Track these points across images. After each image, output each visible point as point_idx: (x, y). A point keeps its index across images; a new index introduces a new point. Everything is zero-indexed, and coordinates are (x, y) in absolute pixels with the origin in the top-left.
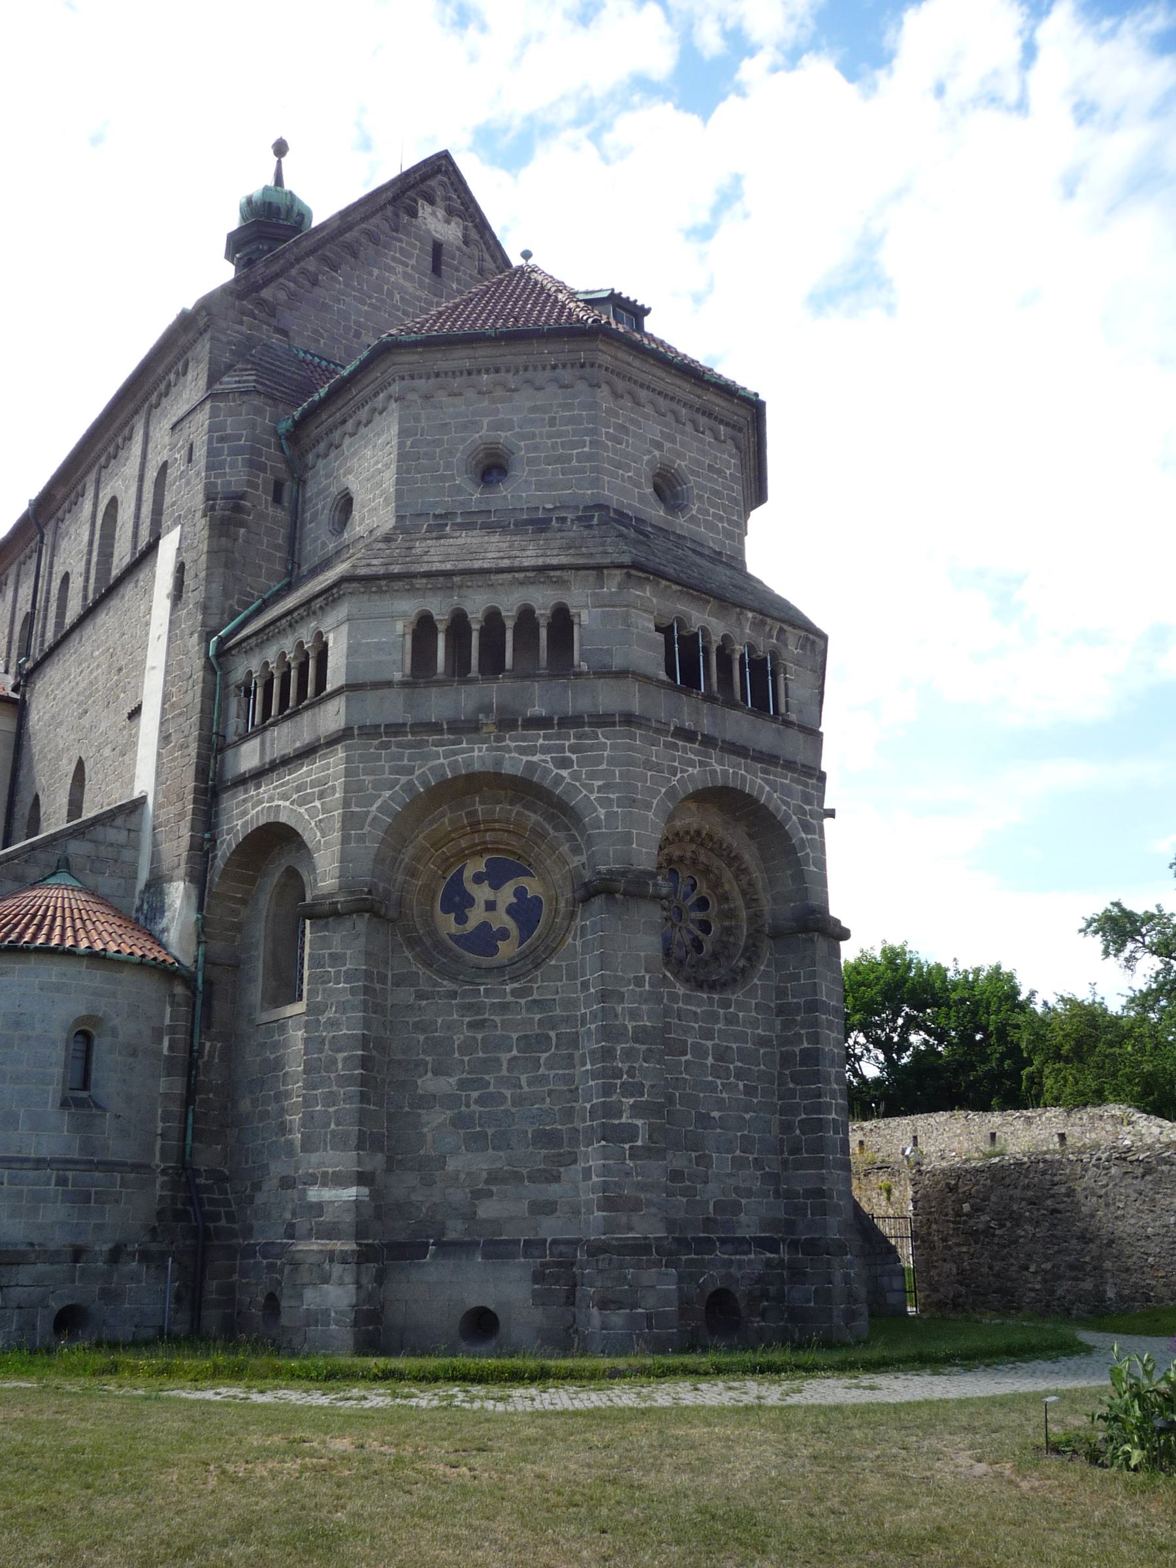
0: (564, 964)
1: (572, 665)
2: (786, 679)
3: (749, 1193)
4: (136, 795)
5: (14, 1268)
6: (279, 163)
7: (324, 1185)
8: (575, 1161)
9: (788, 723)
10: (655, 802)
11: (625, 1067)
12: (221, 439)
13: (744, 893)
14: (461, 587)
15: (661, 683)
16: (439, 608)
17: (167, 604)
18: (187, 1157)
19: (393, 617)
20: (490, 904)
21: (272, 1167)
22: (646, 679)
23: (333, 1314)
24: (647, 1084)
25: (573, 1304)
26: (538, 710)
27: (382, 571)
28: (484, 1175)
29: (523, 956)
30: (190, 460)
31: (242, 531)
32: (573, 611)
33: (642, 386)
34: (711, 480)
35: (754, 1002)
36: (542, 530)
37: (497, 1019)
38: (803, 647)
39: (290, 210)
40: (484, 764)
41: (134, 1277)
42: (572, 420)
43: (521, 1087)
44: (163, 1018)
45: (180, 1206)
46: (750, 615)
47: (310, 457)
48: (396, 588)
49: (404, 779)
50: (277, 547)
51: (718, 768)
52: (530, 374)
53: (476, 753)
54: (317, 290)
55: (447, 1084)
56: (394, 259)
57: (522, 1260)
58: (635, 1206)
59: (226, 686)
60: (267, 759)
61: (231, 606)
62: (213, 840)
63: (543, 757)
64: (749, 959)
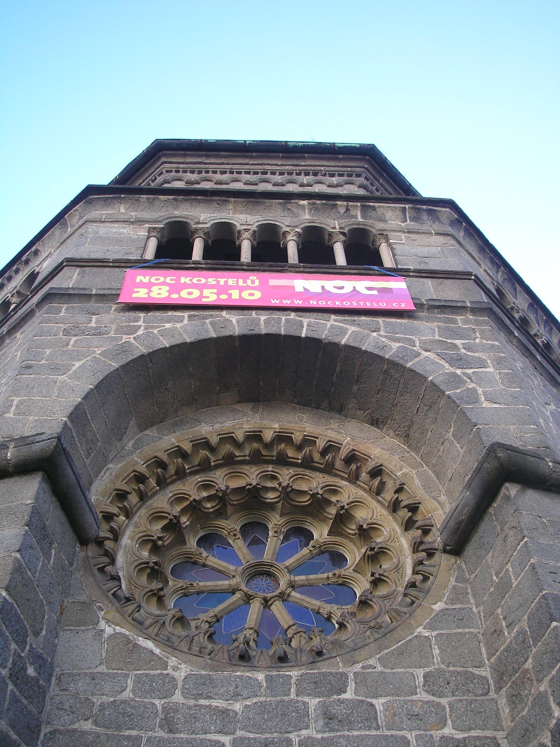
46: (305, 202)
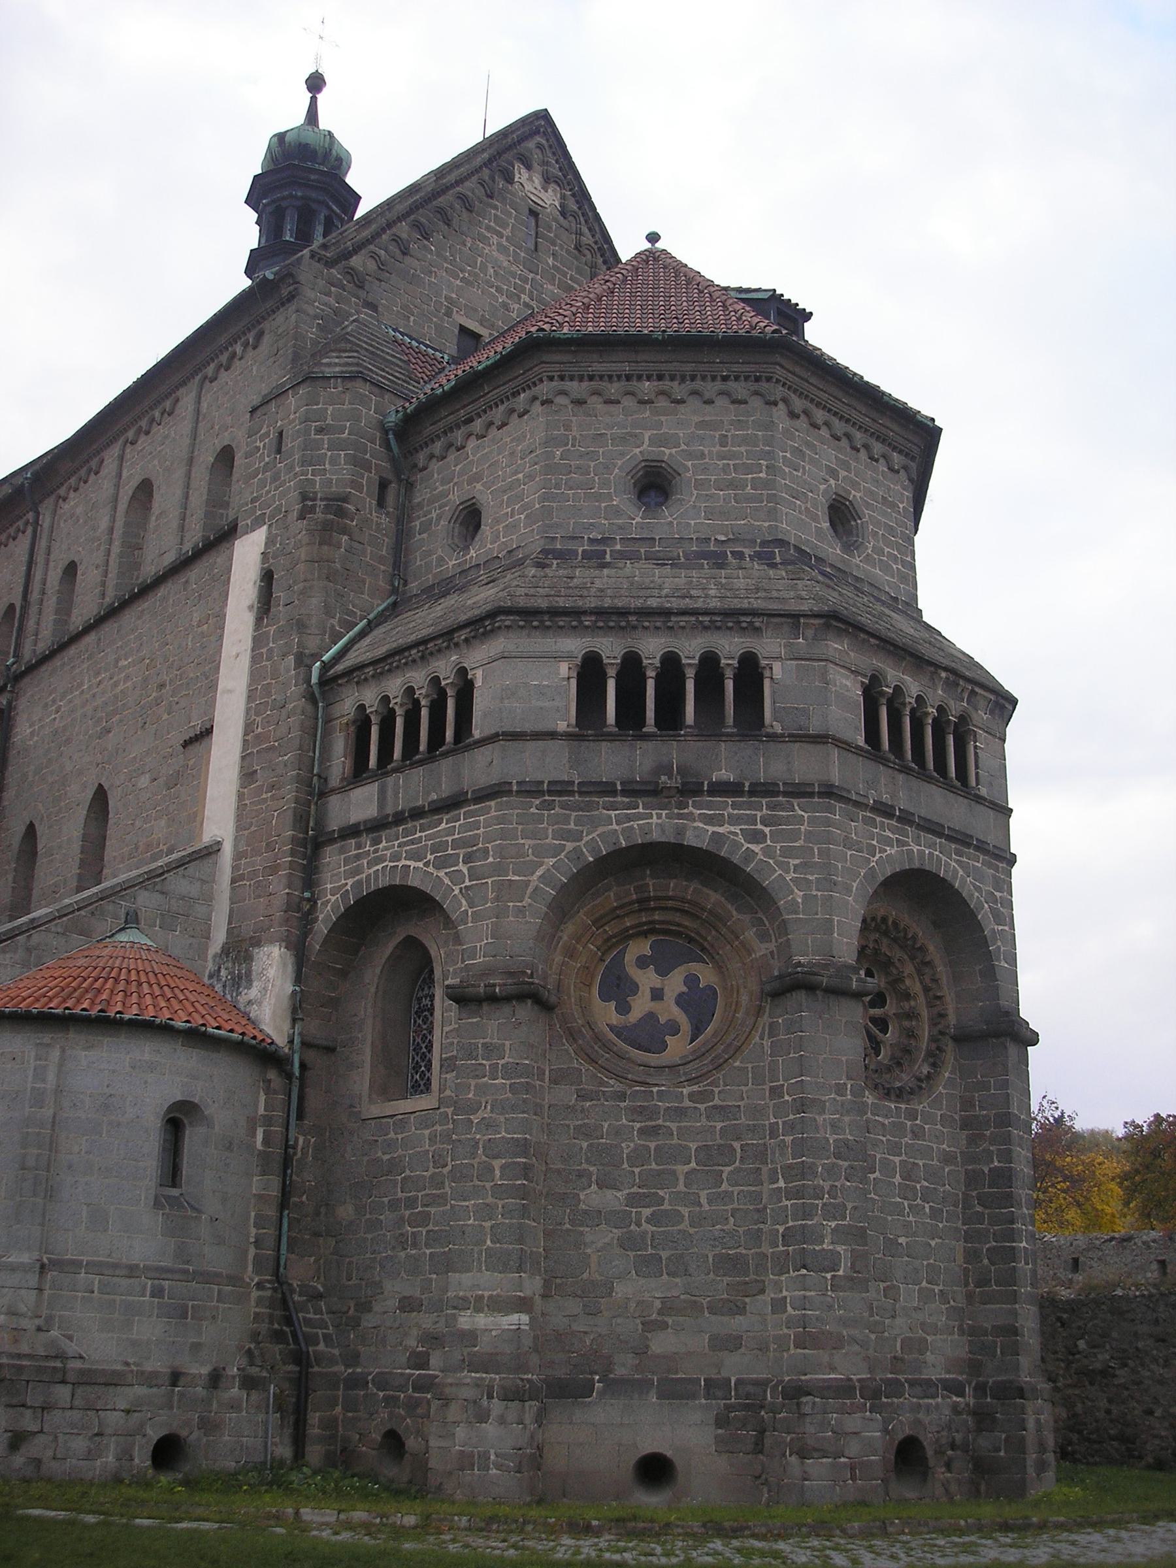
0: (750, 1066)
1: (763, 725)
2: (976, 747)
3: (935, 1330)
4: (207, 839)
5: (111, 1389)
6: (314, 101)
7: (478, 1310)
8: (762, 1291)
9: (979, 799)
10: (855, 885)
11: (827, 1186)
12: (320, 431)
13: (926, 990)
14: (635, 628)
16: (611, 649)
17: (249, 618)
18: (281, 1269)
19: (558, 658)
20: (657, 991)
21: (388, 1285)
22: (844, 745)
23: (492, 1457)
24: (850, 1206)
25: (761, 1452)
26: (724, 774)
27: (543, 604)
28: (658, 1304)
29: (699, 1056)
30: (279, 451)
31: (346, 537)
32: (763, 662)
33: (818, 405)
34: (885, 514)
35: (939, 1113)
36: (721, 566)
37: (673, 1126)
38: (992, 712)
39: (327, 153)
40: (663, 831)
41: (234, 1406)
42: (745, 440)
43: (700, 1205)
44: (256, 1106)
45: (276, 1326)
46: (944, 675)
47: (421, 458)
48: (561, 623)
49: (570, 846)
50: (381, 559)
51: (915, 848)
52: (698, 385)
53: (655, 820)
54: (408, 260)
55: (614, 1199)
56: (488, 228)
57: (703, 1401)
58: (837, 1343)
59: (328, 721)
60: (390, 810)
61: (333, 626)
62: (313, 901)
63: (732, 829)
64: (934, 1065)
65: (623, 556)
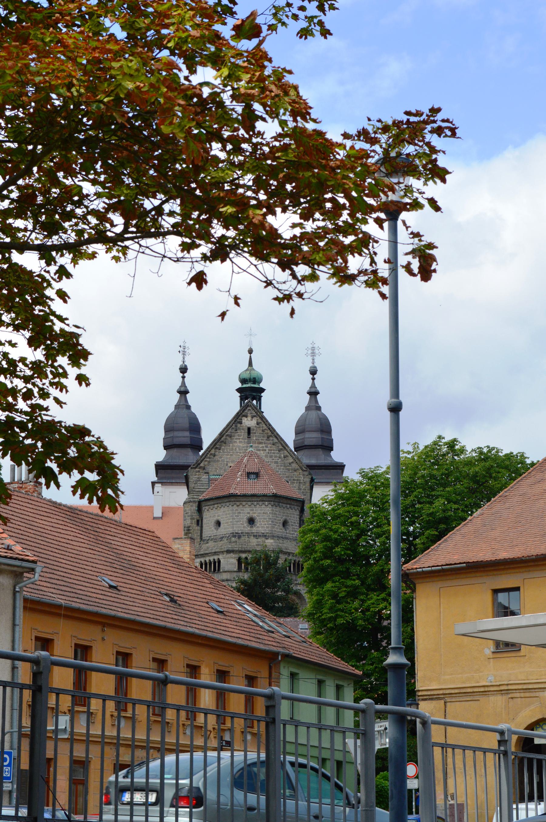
15: (234, 572)
42: (229, 514)
54: (216, 457)
65: (212, 540)
